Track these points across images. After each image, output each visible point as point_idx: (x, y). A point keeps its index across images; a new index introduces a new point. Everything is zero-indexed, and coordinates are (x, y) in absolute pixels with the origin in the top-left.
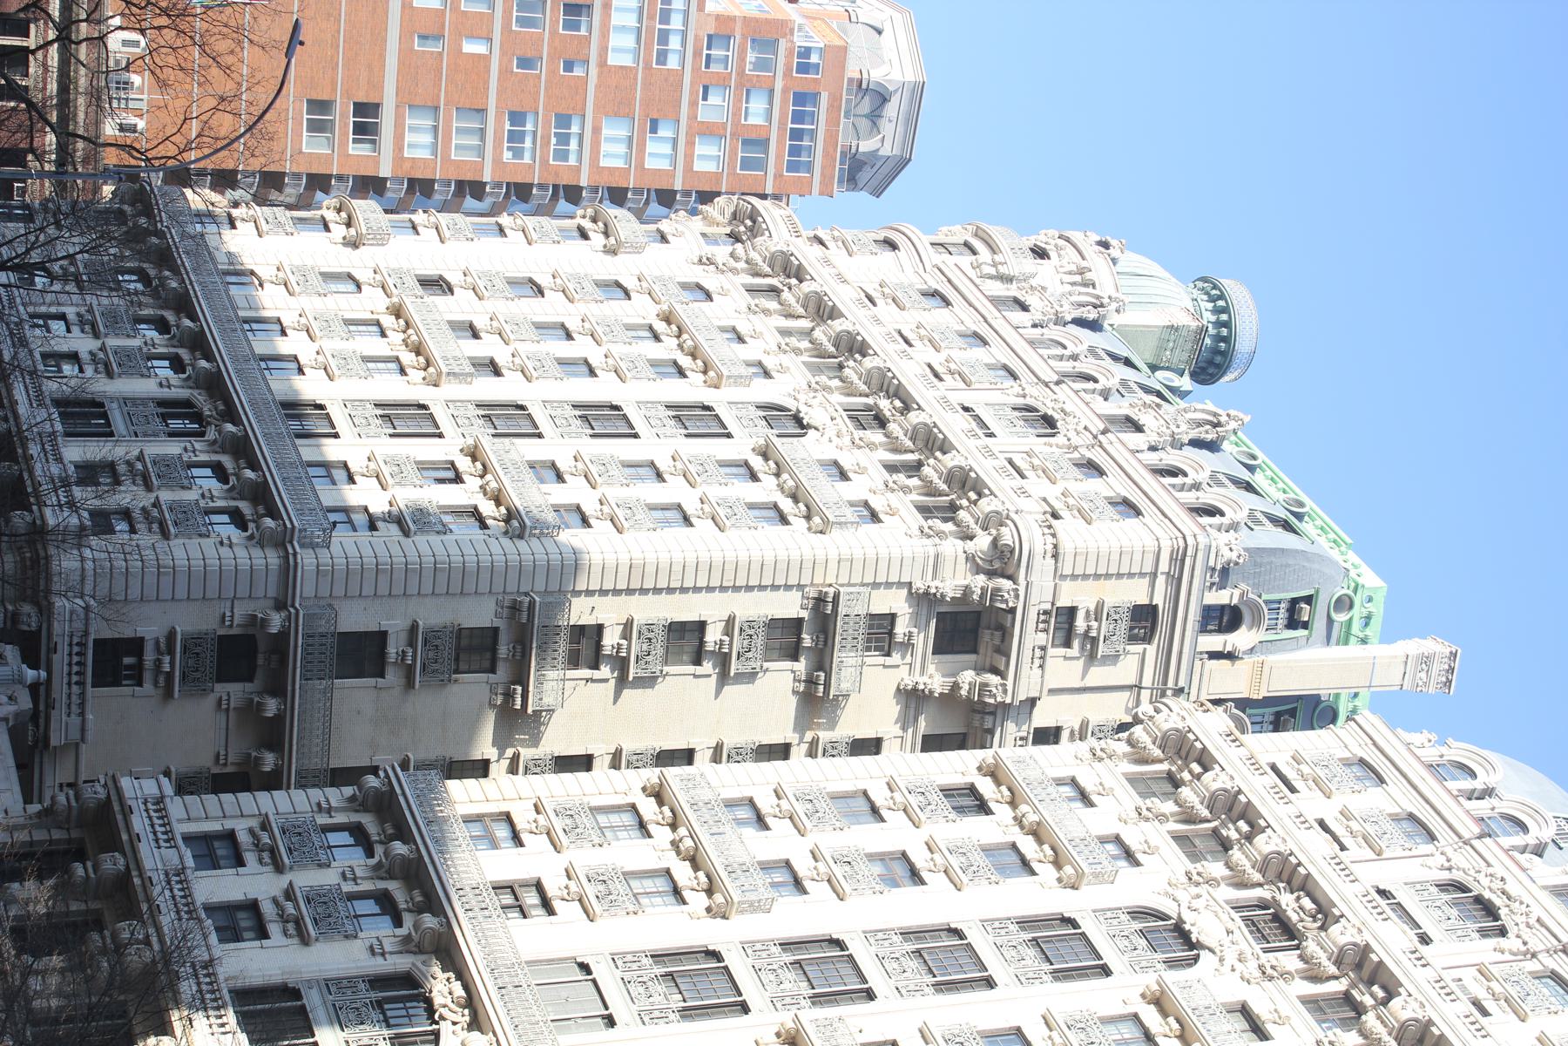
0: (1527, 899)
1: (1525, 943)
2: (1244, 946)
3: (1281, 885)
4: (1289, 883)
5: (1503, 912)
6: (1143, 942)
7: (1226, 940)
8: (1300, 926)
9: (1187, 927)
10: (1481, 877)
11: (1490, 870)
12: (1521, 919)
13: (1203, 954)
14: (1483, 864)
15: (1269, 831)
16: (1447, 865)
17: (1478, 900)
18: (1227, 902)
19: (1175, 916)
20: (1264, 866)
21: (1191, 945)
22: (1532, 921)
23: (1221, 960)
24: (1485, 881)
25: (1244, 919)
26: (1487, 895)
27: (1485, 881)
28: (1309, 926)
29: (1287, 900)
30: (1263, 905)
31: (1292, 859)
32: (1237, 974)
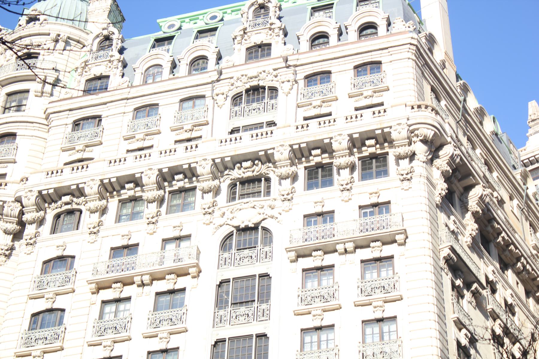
0: (261, 70)
1: (289, 81)
2: (266, 204)
3: (226, 172)
4: (226, 168)
5: (261, 84)
6: (246, 252)
7: (258, 210)
8: (255, 173)
9: (242, 226)
10: (237, 84)
11: (235, 78)
14: (228, 80)
15: (192, 165)
16: (225, 96)
17: (247, 91)
18: (227, 202)
20: (39, 209)
21: (255, 228)
22: (275, 73)
23: (272, 217)
25: (239, 199)
27: (239, 84)
28: (260, 169)
29: (237, 173)
30: (233, 186)
31: (106, 181)
32: (283, 213)
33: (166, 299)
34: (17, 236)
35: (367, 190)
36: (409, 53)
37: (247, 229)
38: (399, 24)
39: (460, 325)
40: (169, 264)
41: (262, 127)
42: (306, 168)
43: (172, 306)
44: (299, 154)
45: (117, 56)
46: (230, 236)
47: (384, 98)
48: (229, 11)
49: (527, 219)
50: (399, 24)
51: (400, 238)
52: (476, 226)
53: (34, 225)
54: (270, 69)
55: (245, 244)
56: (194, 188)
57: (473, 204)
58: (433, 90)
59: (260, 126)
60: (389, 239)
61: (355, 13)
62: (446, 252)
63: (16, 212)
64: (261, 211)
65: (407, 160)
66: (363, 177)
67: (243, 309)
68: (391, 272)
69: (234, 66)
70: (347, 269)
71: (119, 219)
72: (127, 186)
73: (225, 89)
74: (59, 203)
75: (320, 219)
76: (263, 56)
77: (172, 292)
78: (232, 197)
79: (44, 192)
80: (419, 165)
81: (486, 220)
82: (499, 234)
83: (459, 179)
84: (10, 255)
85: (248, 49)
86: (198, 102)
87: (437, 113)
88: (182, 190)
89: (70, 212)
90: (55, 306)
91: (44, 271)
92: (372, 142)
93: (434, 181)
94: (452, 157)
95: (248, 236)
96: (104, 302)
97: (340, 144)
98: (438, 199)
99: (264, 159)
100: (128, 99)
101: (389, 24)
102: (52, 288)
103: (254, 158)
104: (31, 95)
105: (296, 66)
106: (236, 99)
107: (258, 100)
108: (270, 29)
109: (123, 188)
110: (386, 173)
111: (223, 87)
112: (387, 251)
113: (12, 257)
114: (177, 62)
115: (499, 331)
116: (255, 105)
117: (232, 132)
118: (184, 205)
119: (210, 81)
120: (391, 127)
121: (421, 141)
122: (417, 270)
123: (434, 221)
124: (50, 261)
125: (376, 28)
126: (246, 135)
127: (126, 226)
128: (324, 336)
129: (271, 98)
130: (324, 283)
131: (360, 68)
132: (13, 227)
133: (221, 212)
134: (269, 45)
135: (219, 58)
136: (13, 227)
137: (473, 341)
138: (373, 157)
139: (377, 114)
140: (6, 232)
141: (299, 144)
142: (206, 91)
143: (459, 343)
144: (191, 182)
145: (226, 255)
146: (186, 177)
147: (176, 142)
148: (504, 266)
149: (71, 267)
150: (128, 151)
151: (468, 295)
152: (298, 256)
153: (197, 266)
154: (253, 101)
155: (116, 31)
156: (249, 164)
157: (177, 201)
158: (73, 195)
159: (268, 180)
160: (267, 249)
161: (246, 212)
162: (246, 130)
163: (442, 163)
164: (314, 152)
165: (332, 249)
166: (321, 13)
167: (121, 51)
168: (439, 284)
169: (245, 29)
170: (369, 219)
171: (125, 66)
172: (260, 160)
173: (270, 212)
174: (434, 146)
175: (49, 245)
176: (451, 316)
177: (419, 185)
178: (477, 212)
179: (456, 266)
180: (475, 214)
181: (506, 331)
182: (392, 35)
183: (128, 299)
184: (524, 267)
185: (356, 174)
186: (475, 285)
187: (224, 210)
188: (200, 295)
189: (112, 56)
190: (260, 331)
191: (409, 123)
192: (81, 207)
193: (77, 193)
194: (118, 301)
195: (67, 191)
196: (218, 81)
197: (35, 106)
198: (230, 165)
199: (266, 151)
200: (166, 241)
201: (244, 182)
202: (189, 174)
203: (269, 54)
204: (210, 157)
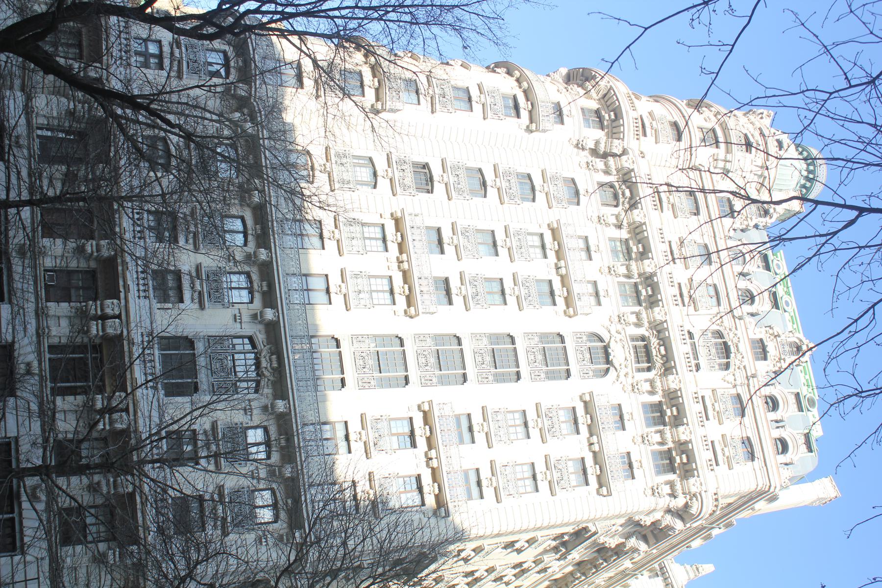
0: (745, 355)
4: (659, 332)
5: (732, 355)
6: (588, 356)
9: (610, 351)
11: (736, 332)
12: (738, 363)
17: (725, 343)
19: (607, 341)
21: (608, 361)
22: (742, 367)
23: (618, 376)
24: (732, 335)
26: (730, 343)
27: (732, 335)
28: (658, 361)
29: (654, 342)
30: (643, 339)
32: (622, 386)
33: (547, 289)
34: (594, 152)
35: (644, 457)
36: (762, 484)
37: (607, 354)
38: (787, 473)
39: (531, 542)
40: (576, 288)
41: (695, 359)
42: (660, 402)
43: (540, 295)
44: (673, 397)
45: (752, 224)
46: (601, 340)
47: (723, 467)
48: (795, 326)
49: (617, 574)
50: (787, 473)
51: (604, 490)
52: (613, 546)
53: (603, 167)
54: (745, 363)
55: (595, 353)
56: (640, 305)
57: (633, 542)
58: (730, 504)
59: (696, 358)
60: (603, 481)
61: (795, 432)
62: (593, 529)
63: (615, 151)
64: (623, 366)
65: (669, 492)
66: (654, 453)
67: (540, 357)
68: (574, 483)
69: (746, 329)
70: (575, 446)
71: (611, 239)
74: (623, 187)
75: (618, 418)
77: (552, 293)
78: (633, 339)
79: (633, 174)
80: (665, 501)
81: (619, 551)
82: (605, 560)
83: (653, 533)
84: (578, 148)
85: (761, 340)
86: (714, 299)
87: (711, 515)
88: (638, 293)
90: (537, 193)
91: (565, 180)
92: (685, 460)
93: (651, 515)
94: (673, 528)
95: (601, 355)
96: (542, 235)
97: (683, 433)
98: (637, 518)
99: (667, 365)
100: (715, 237)
101: (786, 464)
102: (552, 189)
103: (668, 358)
104: (715, 151)
105: (748, 386)
106: (719, 334)
107: (718, 353)
108: (780, 359)
110: (658, 473)
112: (593, 480)
113: (576, 150)
114: (748, 277)
115: (525, 566)
116: (713, 351)
117: (689, 333)
118: (626, 296)
120: (698, 476)
121: (687, 503)
122: (578, 506)
123: (619, 516)
124: (575, 184)
125: (782, 453)
126: (688, 348)
127: (605, 247)
128: (521, 430)
129: (720, 365)
130: (563, 426)
131: (747, 442)
132: (602, 149)
133: (621, 330)
134: (765, 359)
135: (752, 315)
136: (602, 149)
137: (519, 551)
138: (671, 460)
139: (709, 463)
140: (597, 143)
141: (681, 396)
143: (517, 541)
144: (645, 301)
145: (585, 338)
146: (650, 296)
147: (679, 284)
148: (579, 564)
149: (570, 203)
151: (554, 543)
152: (585, 403)
153: (575, 314)
154: (717, 349)
155: (773, 220)
156: (663, 352)
157: (629, 290)
158: (631, 199)
159: (649, 369)
160: (591, 373)
161: (621, 353)
162: (691, 345)
163: (668, 520)
165: (594, 431)
166: (794, 401)
167: (756, 226)
168: (567, 525)
169: (779, 336)
170: (619, 460)
171: (742, 230)
172: (667, 361)
173: (622, 374)
174: (682, 514)
175: (587, 181)
176: (539, 534)
177: (649, 502)
178: (625, 547)
179: (580, 535)
180: (623, 544)
181: (524, 572)
182: (778, 468)
183: (545, 257)
184: (577, 579)
185: (657, 447)
186: (564, 550)
187: (623, 332)
188: (549, 319)
189: (751, 219)
190: (522, 375)
191: (703, 493)
192: (621, 207)
193: (633, 202)
194: (543, 247)
195: (634, 193)
197: (704, 156)
198: (662, 336)
199: (675, 367)
200: (595, 283)
201: (647, 348)
202: (652, 299)
203: (757, 359)
204: (668, 318)
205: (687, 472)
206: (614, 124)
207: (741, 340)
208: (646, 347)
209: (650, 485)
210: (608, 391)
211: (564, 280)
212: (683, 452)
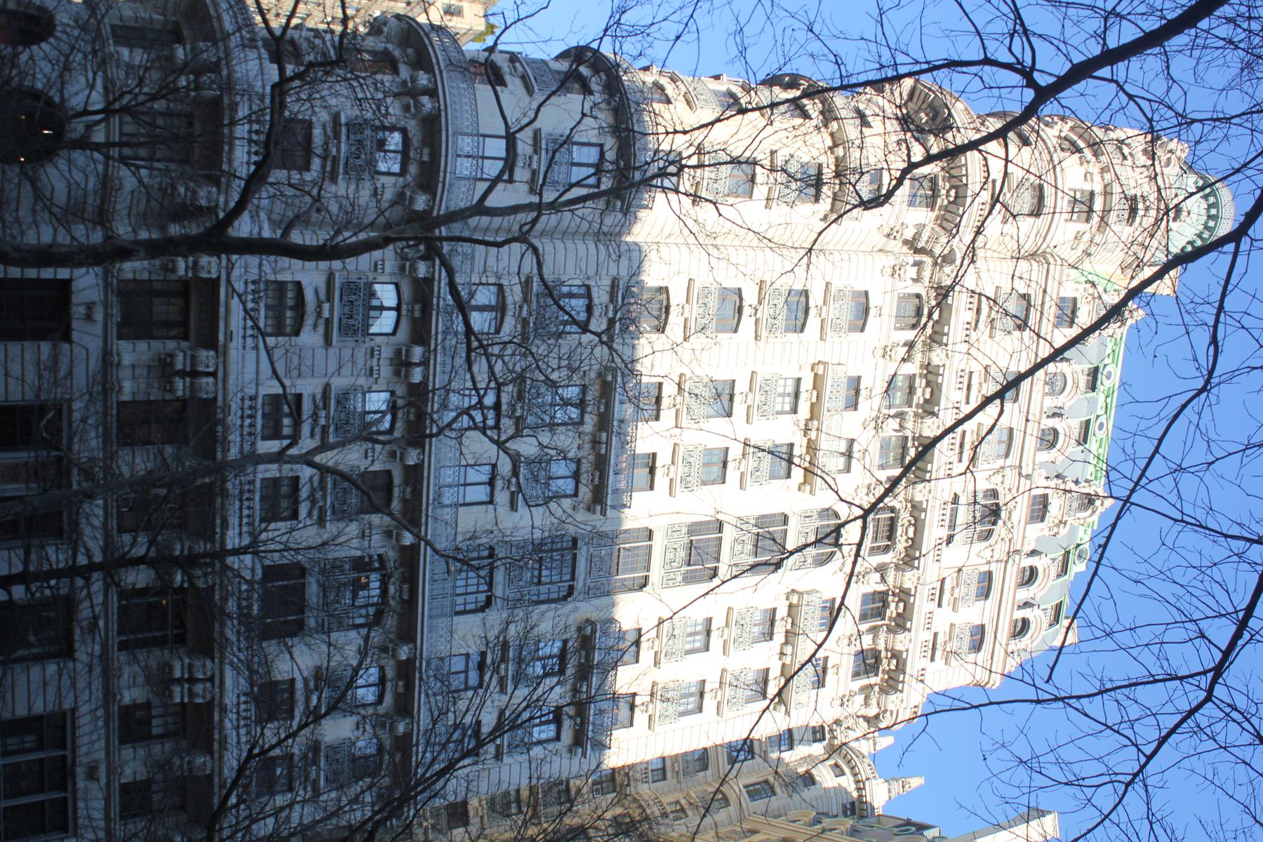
4: (913, 506)
5: (1000, 522)
13: (838, 553)
28: (901, 544)
34: (911, 244)
72: (928, 390)
73: (1007, 484)
76: (1033, 511)
86: (1004, 446)
89: (919, 312)
99: (911, 552)
103: (915, 543)
105: (1007, 562)
106: (994, 493)
109: (928, 384)
110: (856, 675)
111: (1011, 475)
119: (1023, 464)
142: (1013, 459)
150: (936, 635)
156: (911, 535)
159: (886, 549)
164: (901, 605)
196: (1020, 474)
198: (916, 514)
205: (892, 685)
206: (951, 208)
207: (1018, 506)
208: (892, 519)
209: (840, 694)
210: (825, 581)
211: (812, 447)
212: (894, 656)
